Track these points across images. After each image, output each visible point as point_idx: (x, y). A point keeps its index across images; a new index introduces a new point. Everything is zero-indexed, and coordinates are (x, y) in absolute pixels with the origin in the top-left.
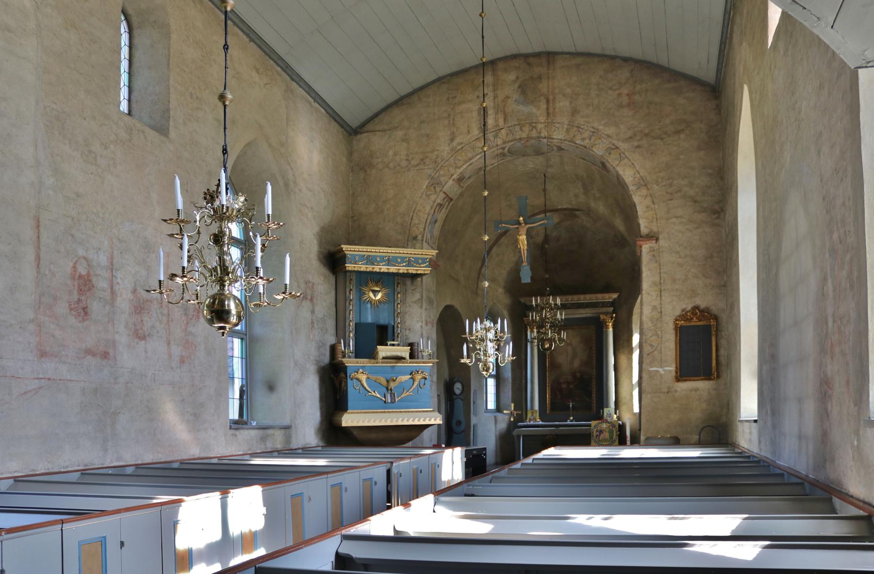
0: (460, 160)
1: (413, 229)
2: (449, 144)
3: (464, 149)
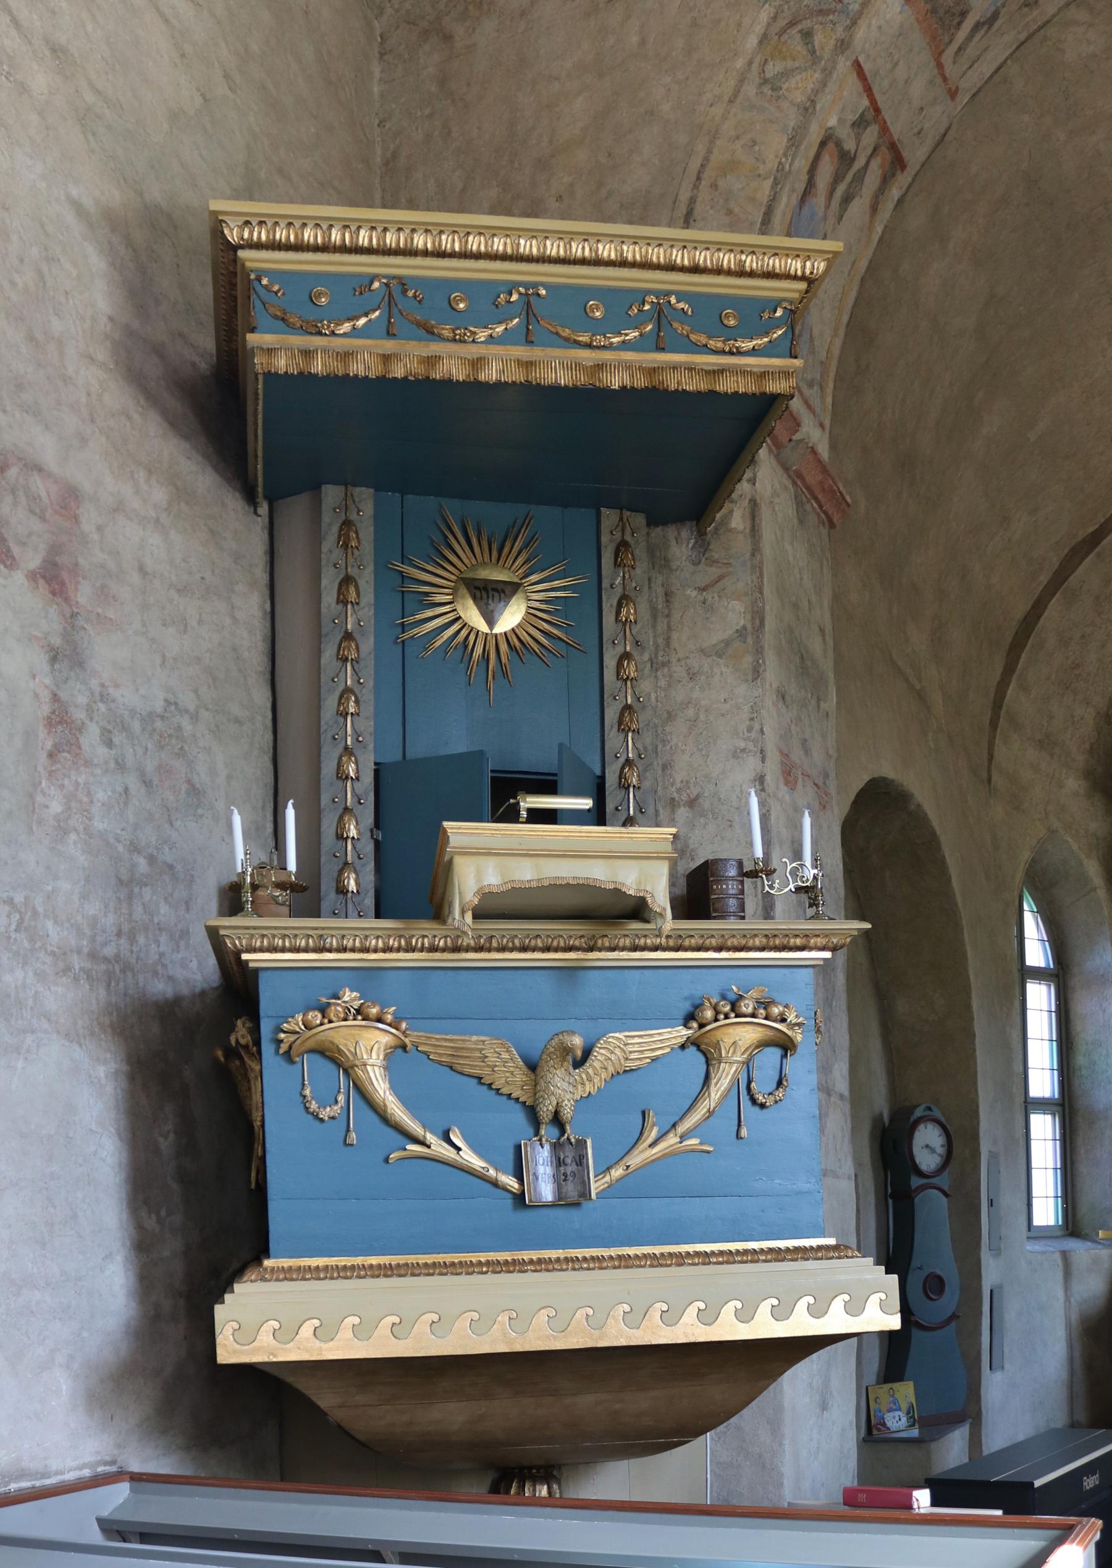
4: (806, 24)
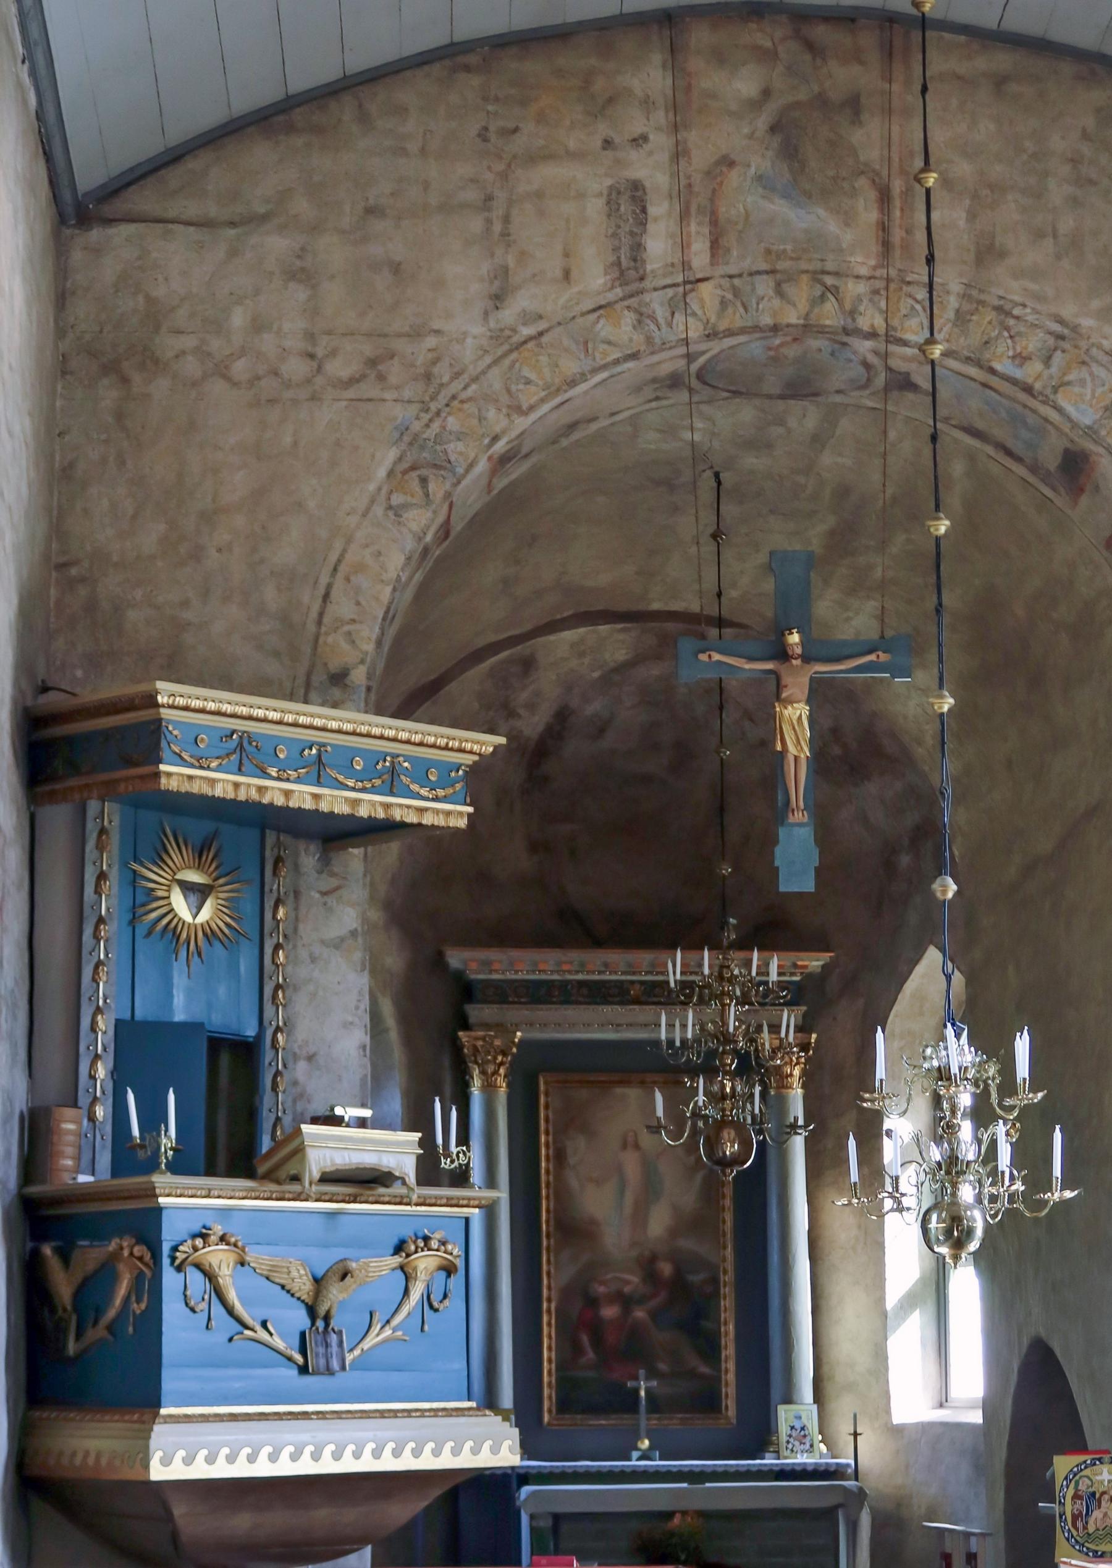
0: (528, 382)
1: (330, 640)
2: (486, 314)
3: (545, 339)
4: (424, 472)
